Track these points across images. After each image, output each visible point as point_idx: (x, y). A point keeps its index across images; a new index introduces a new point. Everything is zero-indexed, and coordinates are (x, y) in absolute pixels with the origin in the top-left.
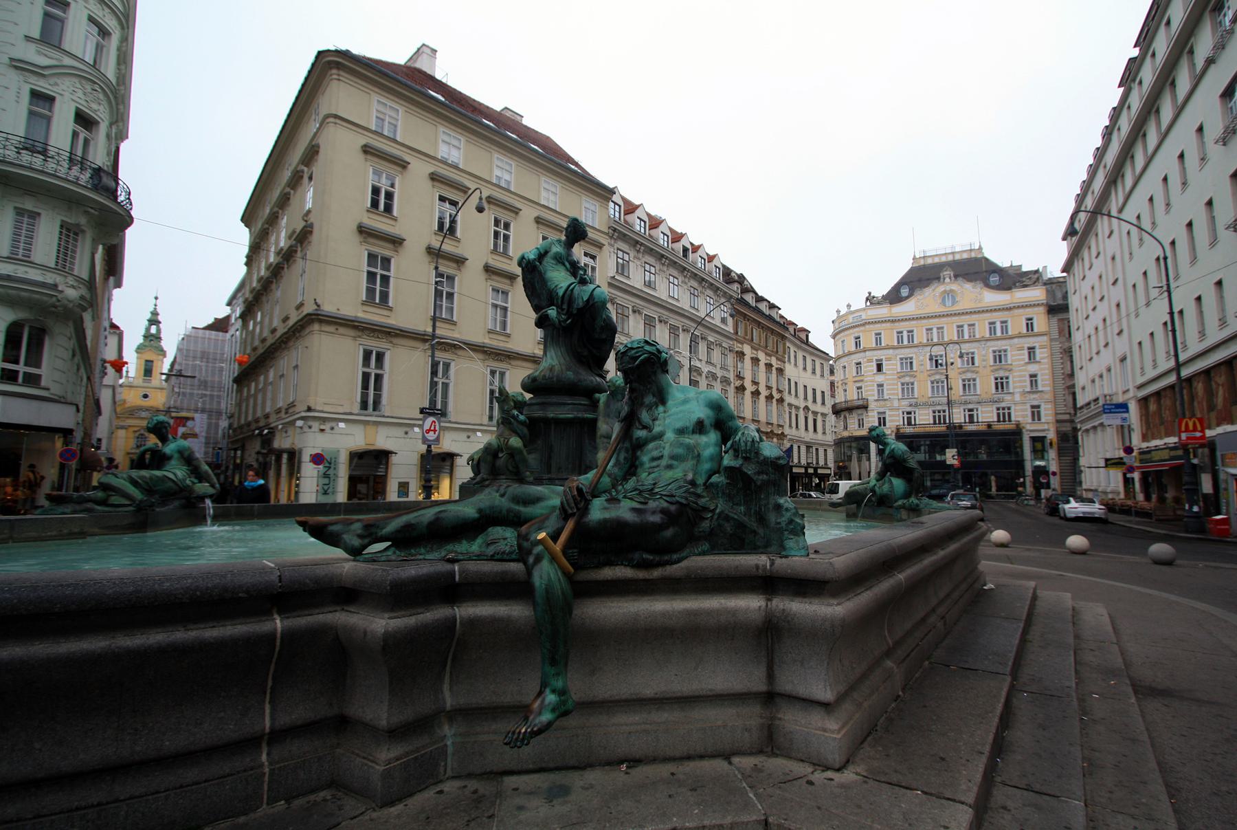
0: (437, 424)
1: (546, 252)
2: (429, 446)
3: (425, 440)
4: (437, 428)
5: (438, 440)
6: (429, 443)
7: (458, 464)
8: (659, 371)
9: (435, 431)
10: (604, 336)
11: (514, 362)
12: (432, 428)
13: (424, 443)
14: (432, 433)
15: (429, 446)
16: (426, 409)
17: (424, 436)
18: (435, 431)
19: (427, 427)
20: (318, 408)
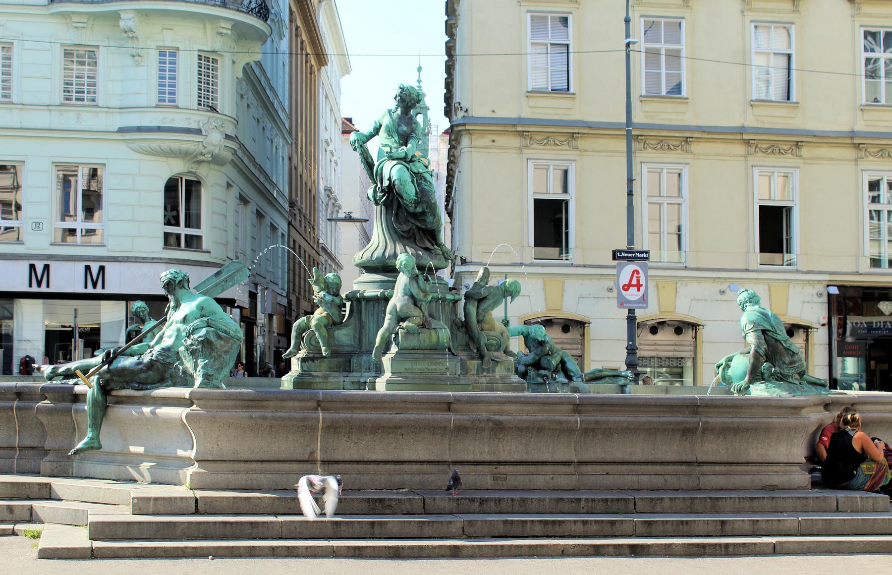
0: (642, 274)
1: (381, 126)
2: (631, 311)
3: (622, 302)
4: (643, 281)
6: (631, 306)
8: (177, 288)
9: (638, 286)
10: (419, 210)
12: (634, 282)
14: (633, 290)
15: (631, 311)
16: (621, 252)
17: (620, 295)
18: (638, 286)
19: (624, 279)
20: (474, 260)
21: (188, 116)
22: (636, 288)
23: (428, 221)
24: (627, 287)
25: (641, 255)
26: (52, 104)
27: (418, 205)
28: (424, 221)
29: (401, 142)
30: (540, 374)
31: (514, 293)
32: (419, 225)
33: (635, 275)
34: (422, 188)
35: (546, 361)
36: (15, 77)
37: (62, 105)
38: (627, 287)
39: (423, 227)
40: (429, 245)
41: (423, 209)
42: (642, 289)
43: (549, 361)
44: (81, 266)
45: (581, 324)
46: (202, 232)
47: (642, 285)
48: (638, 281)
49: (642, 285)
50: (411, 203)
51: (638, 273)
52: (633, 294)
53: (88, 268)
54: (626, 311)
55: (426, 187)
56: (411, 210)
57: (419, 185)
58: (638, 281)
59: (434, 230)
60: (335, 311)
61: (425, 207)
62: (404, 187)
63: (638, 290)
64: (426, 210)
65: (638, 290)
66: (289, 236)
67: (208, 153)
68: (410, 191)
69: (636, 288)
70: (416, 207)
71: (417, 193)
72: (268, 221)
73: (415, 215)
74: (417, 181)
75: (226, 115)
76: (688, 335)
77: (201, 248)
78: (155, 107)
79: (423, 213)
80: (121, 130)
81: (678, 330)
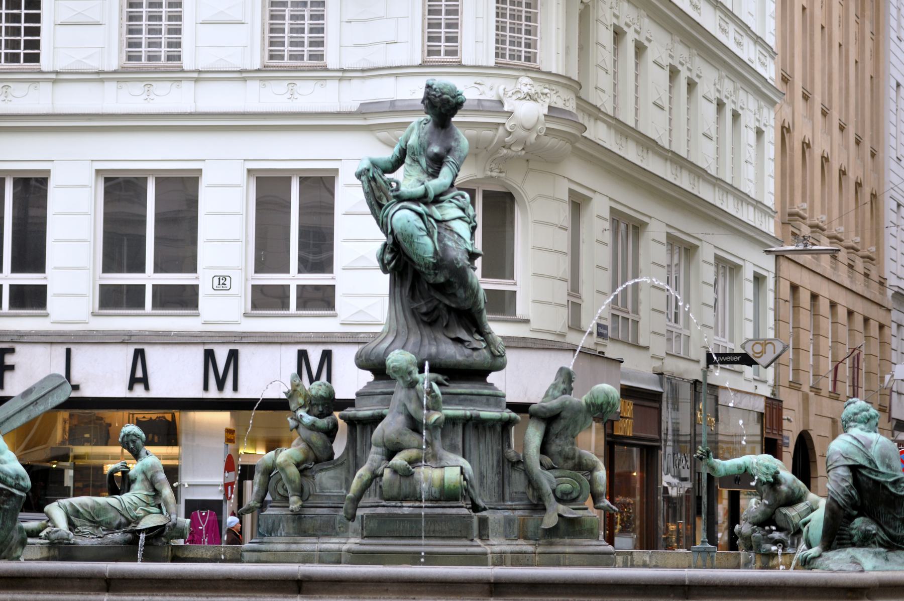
21: (478, 79)
23: (459, 295)
26: (249, 68)
28: (454, 295)
29: (430, 170)
30: (772, 539)
31: (604, 407)
32: (447, 302)
34: (445, 245)
35: (783, 518)
37: (265, 69)
39: (453, 305)
40: (464, 335)
41: (445, 277)
43: (785, 515)
46: (515, 284)
55: (450, 243)
57: (440, 241)
60: (317, 439)
62: (411, 245)
66: (777, 277)
67: (516, 143)
68: (426, 246)
72: (707, 253)
73: (440, 288)
74: (439, 233)
75: (550, 73)
77: (514, 313)
78: (420, 66)
79: (448, 284)
80: (366, 110)
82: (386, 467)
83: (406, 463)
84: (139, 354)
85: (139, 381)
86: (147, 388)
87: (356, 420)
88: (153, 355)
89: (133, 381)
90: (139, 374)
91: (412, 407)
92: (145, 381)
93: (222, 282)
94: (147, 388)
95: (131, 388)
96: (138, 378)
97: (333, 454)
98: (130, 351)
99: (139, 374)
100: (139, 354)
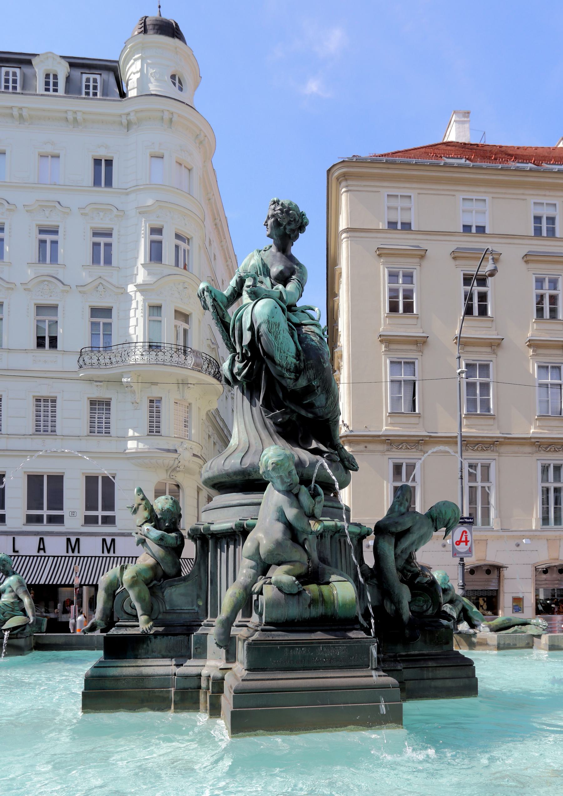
0: (468, 534)
2: (462, 559)
5: (470, 550)
6: (461, 555)
7: (505, 577)
9: (466, 542)
10: (302, 382)
11: (503, 449)
12: (464, 539)
13: (454, 555)
14: (463, 544)
18: (466, 542)
19: (457, 537)
22: (465, 543)
24: (458, 543)
25: (468, 521)
27: (300, 375)
33: (464, 534)
36: (58, 419)
38: (458, 543)
41: (309, 380)
42: (469, 544)
44: (100, 539)
45: (499, 568)
47: (469, 541)
48: (466, 538)
49: (469, 541)
50: (288, 370)
51: (466, 532)
52: (463, 548)
53: (104, 540)
54: (459, 559)
56: (289, 383)
58: (466, 538)
59: (328, 420)
61: (312, 377)
63: (466, 545)
64: (315, 383)
65: (466, 545)
69: (464, 543)
70: (296, 379)
71: (298, 356)
76: (494, 575)
81: (488, 572)
82: (265, 583)
83: (294, 578)
84: (42, 540)
85: (42, 549)
86: (45, 552)
87: (209, 534)
88: (46, 539)
89: (39, 549)
90: (42, 547)
91: (291, 513)
92: (44, 549)
93: (73, 514)
94: (45, 552)
95: (38, 552)
96: (41, 548)
97: (180, 571)
98: (37, 539)
99: (42, 547)
100: (42, 540)
